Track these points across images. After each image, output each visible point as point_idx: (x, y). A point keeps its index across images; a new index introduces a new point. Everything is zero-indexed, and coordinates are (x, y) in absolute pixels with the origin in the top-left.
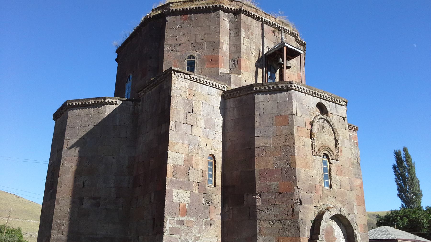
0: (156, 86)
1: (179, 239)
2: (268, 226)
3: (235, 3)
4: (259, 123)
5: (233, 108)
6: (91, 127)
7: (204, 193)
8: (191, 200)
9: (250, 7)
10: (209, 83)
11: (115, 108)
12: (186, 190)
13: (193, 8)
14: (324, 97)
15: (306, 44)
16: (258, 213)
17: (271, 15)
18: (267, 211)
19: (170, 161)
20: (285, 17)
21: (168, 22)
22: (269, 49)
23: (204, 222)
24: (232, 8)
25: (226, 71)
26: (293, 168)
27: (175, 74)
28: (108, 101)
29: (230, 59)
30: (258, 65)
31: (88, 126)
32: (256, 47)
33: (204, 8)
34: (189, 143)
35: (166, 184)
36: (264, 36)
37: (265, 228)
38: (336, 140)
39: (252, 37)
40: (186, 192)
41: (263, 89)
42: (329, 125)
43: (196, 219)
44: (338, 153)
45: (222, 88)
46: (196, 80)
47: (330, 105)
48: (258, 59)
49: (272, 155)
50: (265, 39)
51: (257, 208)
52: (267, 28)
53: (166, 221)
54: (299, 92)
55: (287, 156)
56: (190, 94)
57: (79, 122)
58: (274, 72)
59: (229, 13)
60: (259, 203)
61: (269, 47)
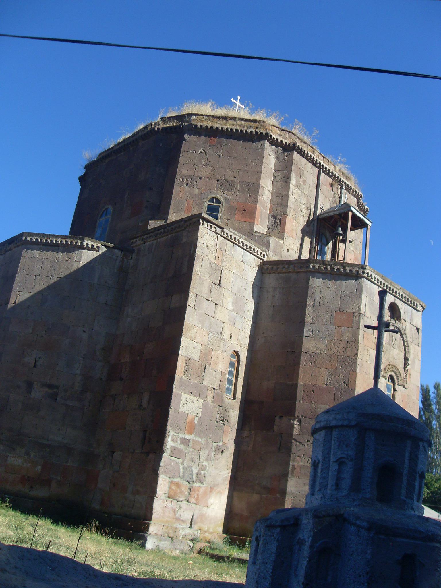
0: (166, 236)
1: (180, 465)
2: (306, 464)
3: (286, 134)
4: (311, 317)
5: (275, 289)
6: (56, 279)
7: (219, 406)
8: (202, 414)
9: (305, 143)
10: (246, 245)
11: (95, 256)
12: (198, 398)
13: (227, 129)
14: (400, 295)
15: (368, 210)
16: (294, 445)
17: (330, 161)
18: (307, 444)
19: (182, 351)
20: (347, 166)
21: (186, 141)
22: (322, 209)
23: (215, 447)
24: (283, 141)
25: (263, 230)
26: (351, 389)
27: (203, 225)
28: (87, 244)
29: (270, 214)
30: (306, 230)
31: (50, 276)
32: (307, 203)
33: (244, 132)
34: (209, 330)
35: (174, 383)
36: (320, 189)
37: (301, 467)
38: (406, 359)
39: (304, 188)
40: (198, 400)
41: (324, 269)
42: (400, 336)
43: (205, 440)
44: (407, 377)
45: (261, 255)
46: (229, 238)
47: (405, 308)
48: (307, 221)
49: (324, 366)
50: (320, 194)
51: (293, 437)
52: (324, 178)
53: (167, 437)
54: (371, 283)
55: (345, 372)
56: (219, 257)
57: (38, 267)
58: (326, 244)
59: (276, 146)
60: (297, 431)
61: (323, 207)
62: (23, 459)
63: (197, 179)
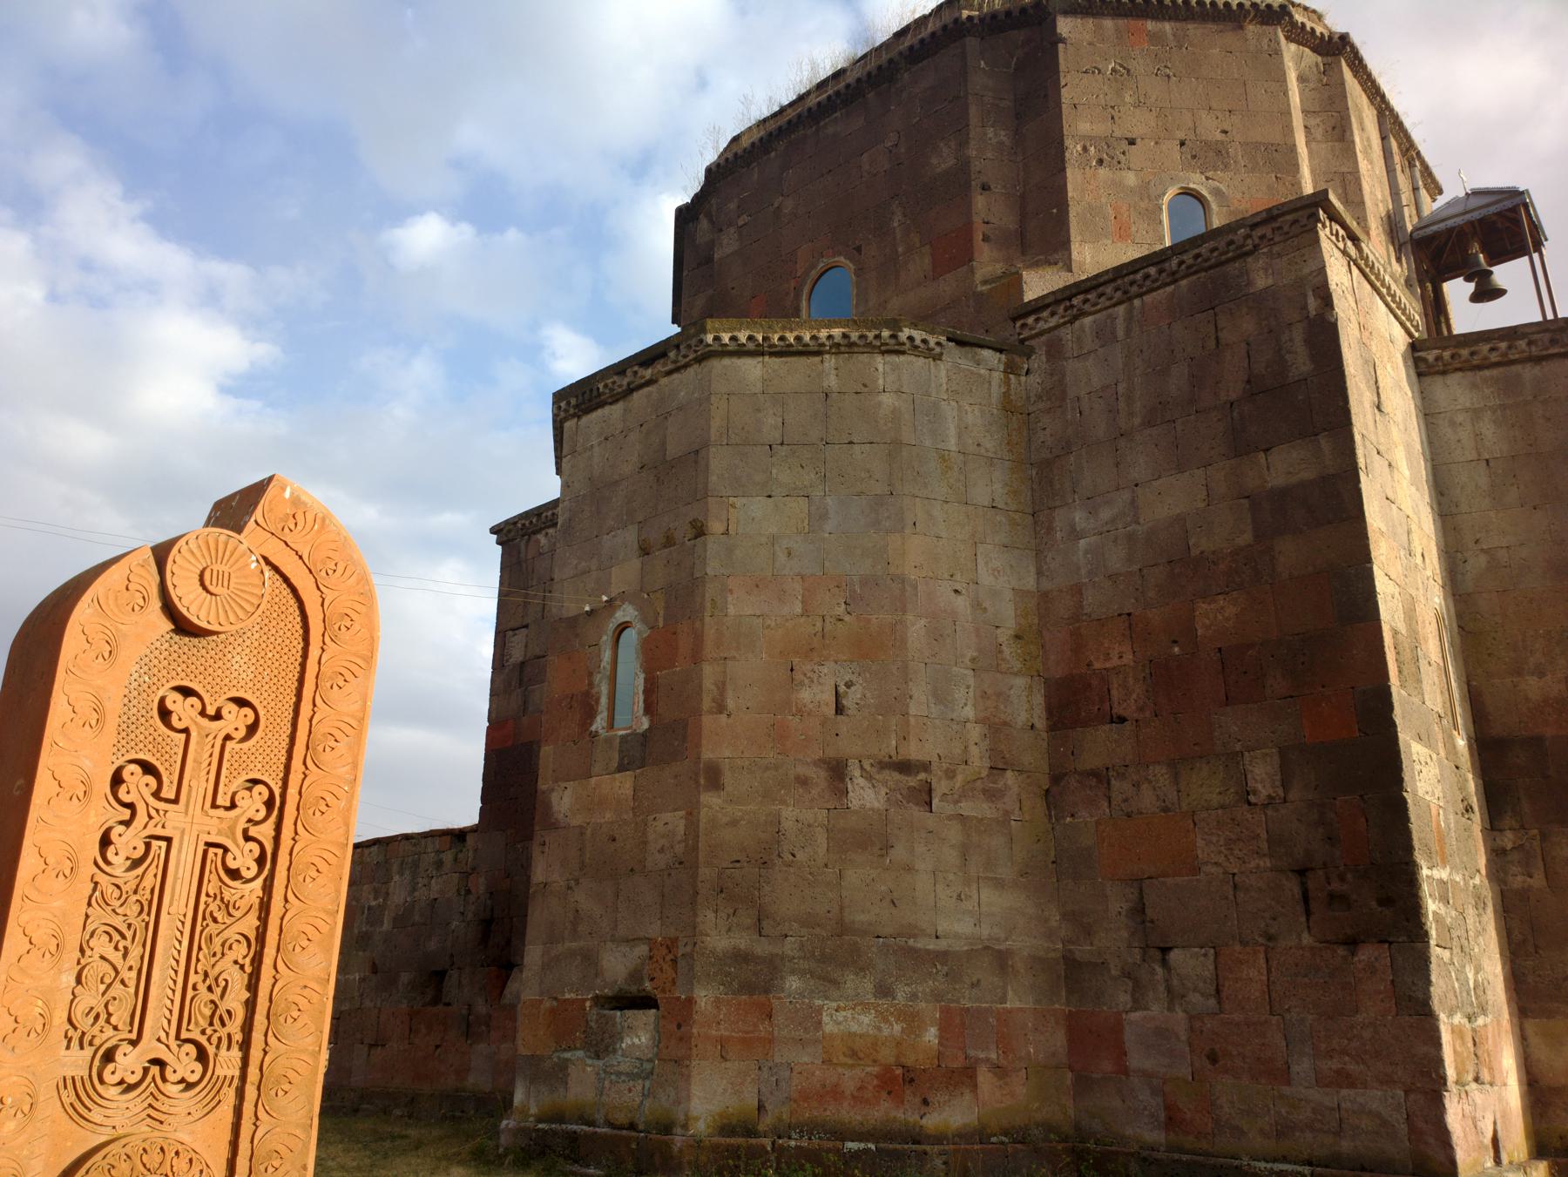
5: (1476, 414)
28: (911, 338)
57: (771, 421)
62: (873, 1011)
63: (1124, 145)
